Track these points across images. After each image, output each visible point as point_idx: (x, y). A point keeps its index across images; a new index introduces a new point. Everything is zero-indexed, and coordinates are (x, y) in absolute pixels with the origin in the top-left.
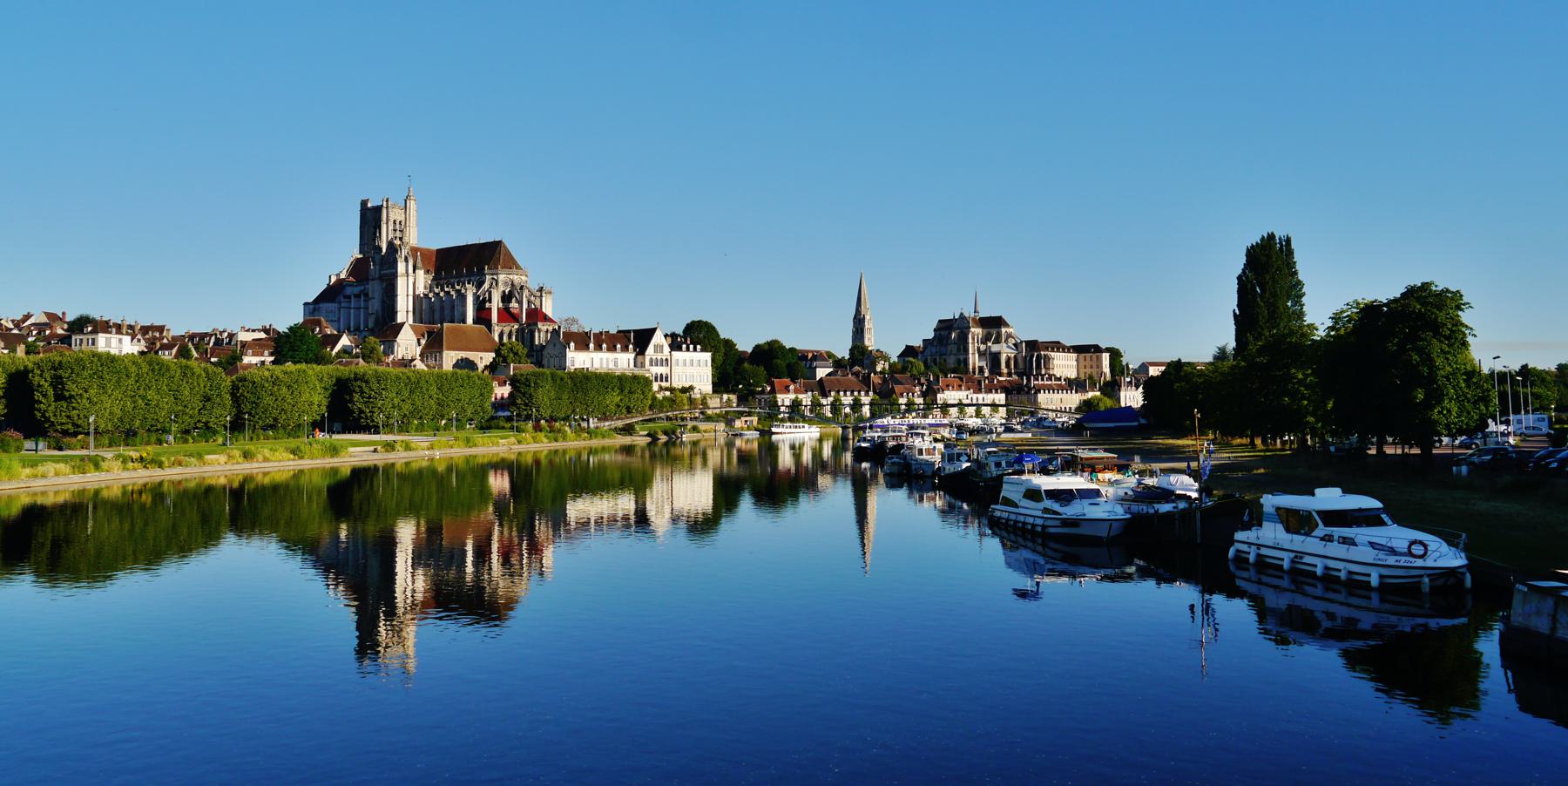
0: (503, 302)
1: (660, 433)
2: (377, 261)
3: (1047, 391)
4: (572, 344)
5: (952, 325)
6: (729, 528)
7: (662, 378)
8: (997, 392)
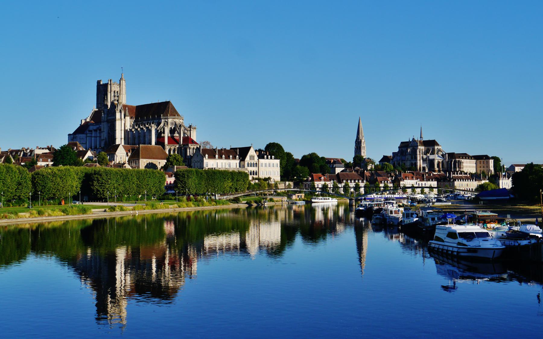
0: (170, 133)
1: (253, 202)
2: (105, 112)
3: (459, 180)
4: (207, 156)
5: (408, 145)
6: (288, 252)
7: (253, 173)
8: (432, 181)
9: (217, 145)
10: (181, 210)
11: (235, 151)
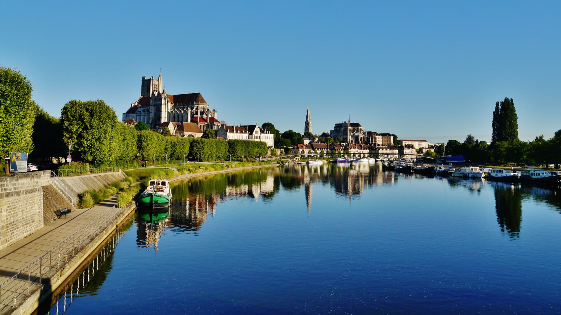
2: (153, 99)
4: (229, 130)
5: (342, 126)
6: (277, 197)
8: (367, 150)
9: (229, 124)
10: (254, 167)
11: (245, 128)
